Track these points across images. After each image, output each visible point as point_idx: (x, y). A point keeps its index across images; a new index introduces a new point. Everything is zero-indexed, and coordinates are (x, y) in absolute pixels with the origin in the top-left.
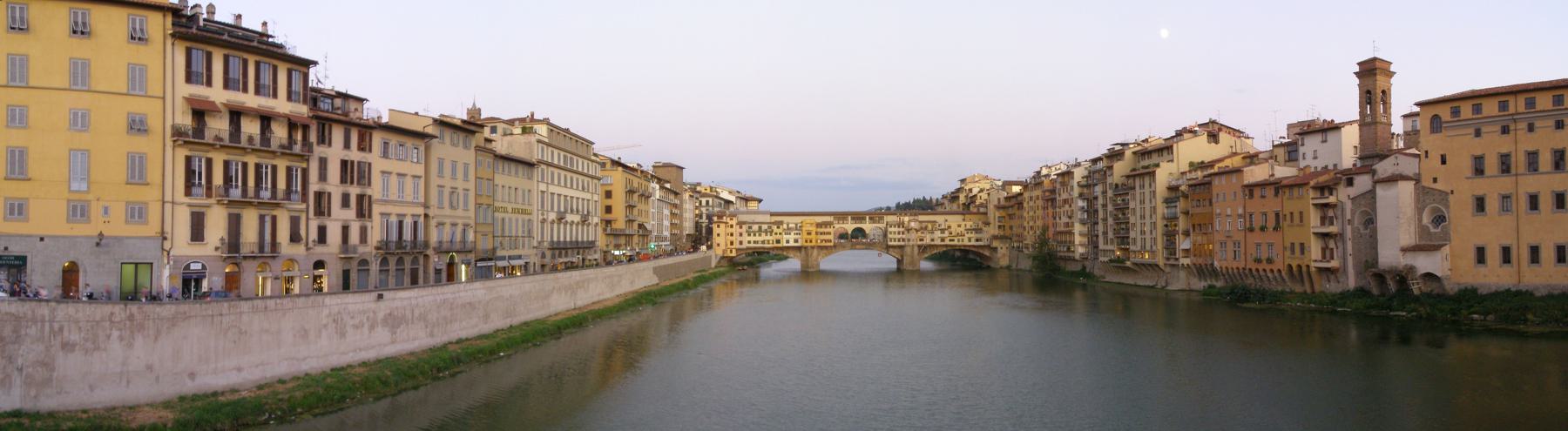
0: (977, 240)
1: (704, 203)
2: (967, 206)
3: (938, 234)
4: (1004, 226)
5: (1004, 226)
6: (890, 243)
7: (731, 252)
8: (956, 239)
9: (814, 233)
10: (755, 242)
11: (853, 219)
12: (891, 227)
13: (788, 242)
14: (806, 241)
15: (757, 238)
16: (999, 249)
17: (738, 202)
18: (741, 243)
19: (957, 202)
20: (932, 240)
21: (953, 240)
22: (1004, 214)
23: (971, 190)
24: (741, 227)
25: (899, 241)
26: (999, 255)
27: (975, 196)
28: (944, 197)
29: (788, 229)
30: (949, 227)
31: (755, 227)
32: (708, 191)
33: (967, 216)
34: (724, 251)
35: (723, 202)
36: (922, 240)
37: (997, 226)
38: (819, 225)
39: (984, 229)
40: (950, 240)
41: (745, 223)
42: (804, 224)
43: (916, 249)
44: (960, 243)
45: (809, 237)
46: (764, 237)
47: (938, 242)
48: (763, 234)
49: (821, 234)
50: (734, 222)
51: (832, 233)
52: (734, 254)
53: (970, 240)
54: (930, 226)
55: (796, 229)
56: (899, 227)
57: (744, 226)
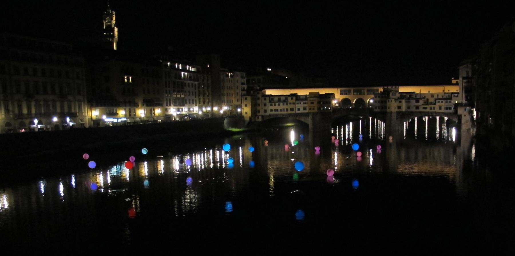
0: (447, 108)
3: (413, 102)
7: (258, 118)
8: (428, 107)
10: (276, 110)
13: (299, 109)
14: (310, 109)
18: (265, 111)
21: (426, 108)
24: (265, 99)
40: (424, 108)
44: (433, 110)
45: (312, 105)
46: (282, 107)
47: (413, 110)
48: (281, 104)
52: (260, 119)
53: (440, 108)
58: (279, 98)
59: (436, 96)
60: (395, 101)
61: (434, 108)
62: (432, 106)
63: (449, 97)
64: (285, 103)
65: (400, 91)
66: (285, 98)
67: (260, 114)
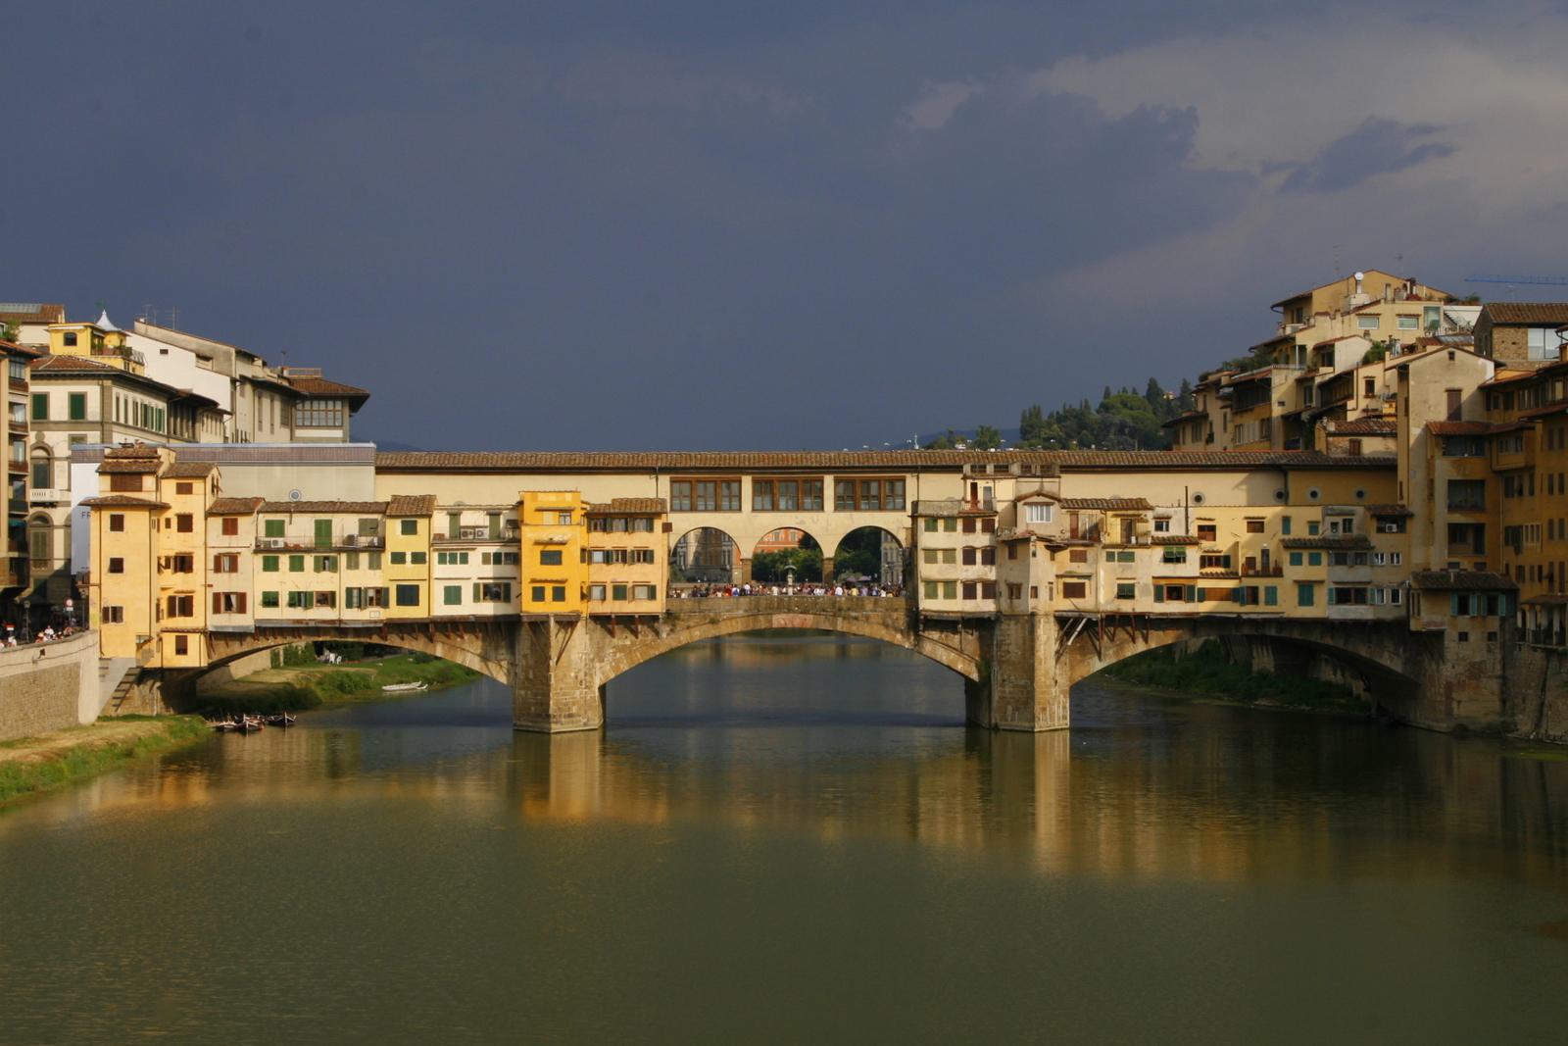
0: (1343, 595)
1: (59, 409)
2: (1298, 427)
3: (1150, 565)
4: (1479, 529)
5: (1479, 529)
6: (926, 604)
7: (182, 649)
9: (571, 554)
10: (298, 599)
11: (759, 488)
12: (932, 522)
13: (453, 595)
14: (538, 595)
15: (312, 580)
16: (1451, 644)
17: (246, 400)
19: (1259, 411)
20: (1126, 592)
22: (1474, 467)
23: (1325, 353)
24: (230, 528)
25: (969, 591)
26: (1448, 672)
27: (1346, 378)
28: (1208, 386)
29: (459, 534)
30: (1208, 531)
31: (300, 529)
32: (82, 350)
33: (1291, 476)
34: (142, 643)
35: (162, 405)
36: (1074, 590)
37: (1441, 533)
38: (599, 519)
39: (1378, 541)
41: (248, 507)
42: (528, 513)
43: (1047, 636)
45: (552, 572)
49: (608, 558)
50: (196, 503)
51: (661, 556)
52: (196, 656)
53: (1306, 590)
54: (1114, 531)
55: (496, 537)
56: (969, 528)
57: (243, 523)
58: (318, 523)
59: (1280, 527)
61: (1272, 596)
62: (1262, 583)
63: (1350, 530)
64: (364, 558)
65: (1063, 496)
66: (360, 520)
67: (196, 620)
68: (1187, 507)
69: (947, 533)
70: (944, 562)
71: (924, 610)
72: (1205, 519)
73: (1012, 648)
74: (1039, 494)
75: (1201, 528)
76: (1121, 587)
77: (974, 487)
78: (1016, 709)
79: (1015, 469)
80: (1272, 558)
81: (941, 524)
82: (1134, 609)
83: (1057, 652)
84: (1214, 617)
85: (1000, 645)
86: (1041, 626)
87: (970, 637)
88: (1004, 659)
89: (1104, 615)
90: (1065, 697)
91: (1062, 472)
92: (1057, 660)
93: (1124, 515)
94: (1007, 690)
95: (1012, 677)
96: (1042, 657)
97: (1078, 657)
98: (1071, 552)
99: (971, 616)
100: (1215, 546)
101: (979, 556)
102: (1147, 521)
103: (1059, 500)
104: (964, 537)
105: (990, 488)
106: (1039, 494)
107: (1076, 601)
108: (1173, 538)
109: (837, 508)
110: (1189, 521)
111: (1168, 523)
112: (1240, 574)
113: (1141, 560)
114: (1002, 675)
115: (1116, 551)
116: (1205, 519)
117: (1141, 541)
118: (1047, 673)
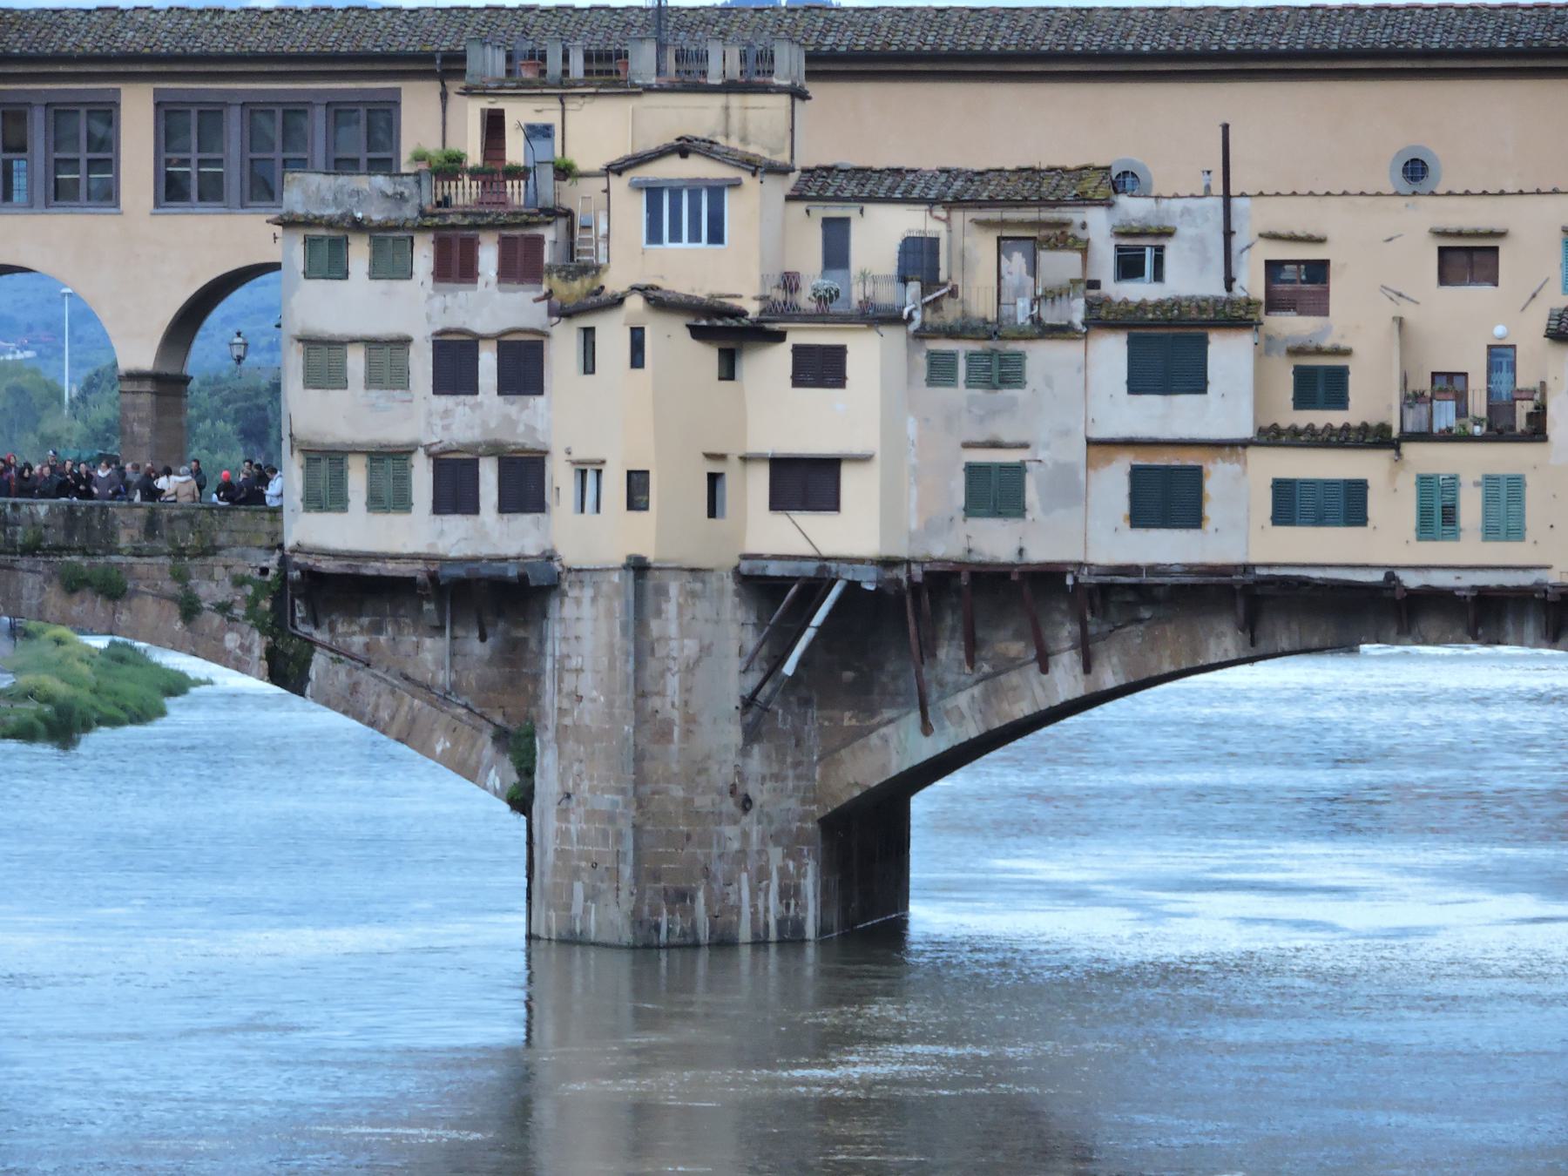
60: (707, 356)
68: (1227, 196)
69: (382, 285)
70: (373, 380)
71: (298, 549)
72: (1293, 239)
73: (587, 684)
74: (683, 148)
75: (1273, 268)
76: (973, 470)
77: (494, 125)
78: (592, 895)
79: (643, 61)
80: (1526, 379)
81: (359, 254)
82: (1021, 551)
83: (748, 702)
84: (1304, 582)
85: (561, 670)
86: (671, 608)
87: (477, 648)
88: (567, 721)
89: (917, 571)
90: (789, 854)
91: (811, 75)
92: (751, 734)
93: (1003, 224)
94: (573, 828)
95: (585, 785)
96: (676, 715)
97: (848, 720)
98: (797, 350)
99: (460, 572)
100: (1326, 331)
101: (488, 360)
102: (1084, 248)
103: (757, 167)
104: (498, 296)
105: (545, 132)
106: (683, 148)
107: (808, 520)
108: (1176, 303)
109: (172, 191)
110: (1238, 243)
111: (1160, 250)
112: (1395, 433)
113: (1049, 382)
114: (562, 778)
115: (961, 348)
116: (1293, 239)
117: (1051, 316)
118: (697, 769)
